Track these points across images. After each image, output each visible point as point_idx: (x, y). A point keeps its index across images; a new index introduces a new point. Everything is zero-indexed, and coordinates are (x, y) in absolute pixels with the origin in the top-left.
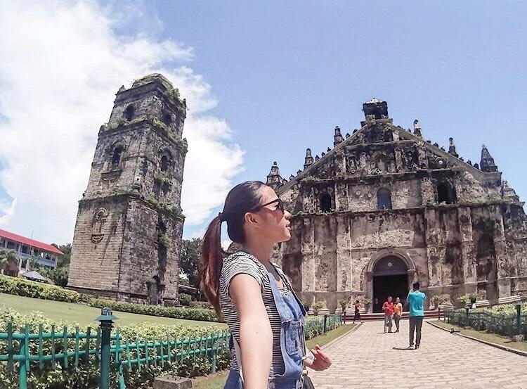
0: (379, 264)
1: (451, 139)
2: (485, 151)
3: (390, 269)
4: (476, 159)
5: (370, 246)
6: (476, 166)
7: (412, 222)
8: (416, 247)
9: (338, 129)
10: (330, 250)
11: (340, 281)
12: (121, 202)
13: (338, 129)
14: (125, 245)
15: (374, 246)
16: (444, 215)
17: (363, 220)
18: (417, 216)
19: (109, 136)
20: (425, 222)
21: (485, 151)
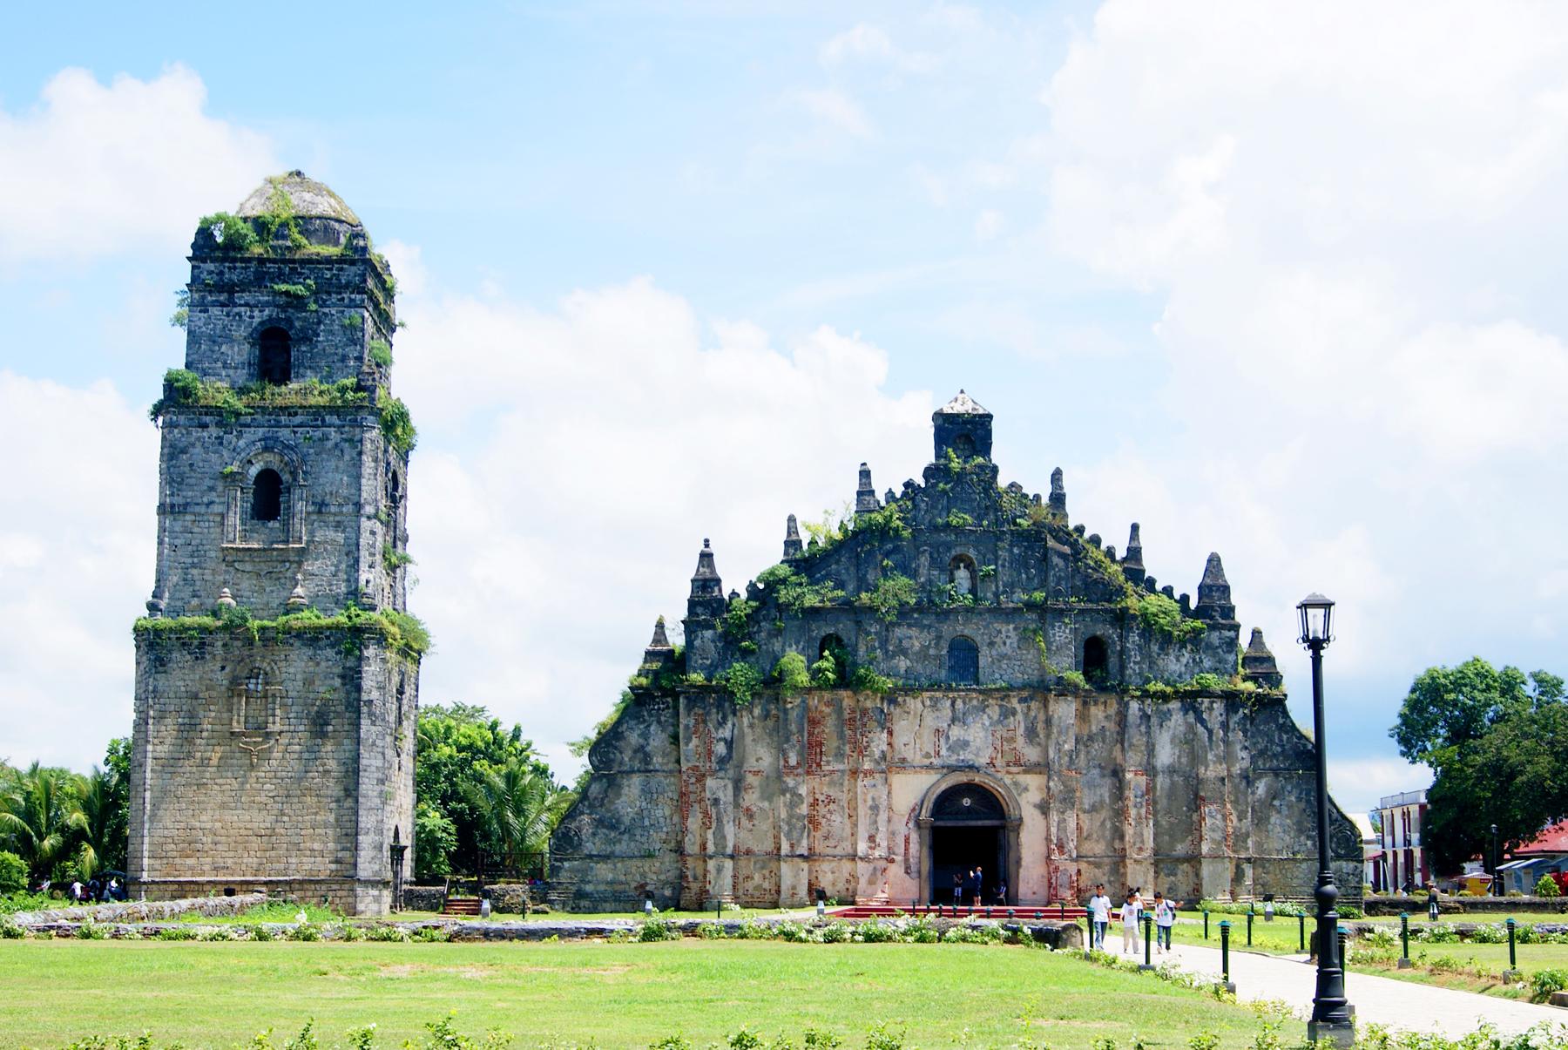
0: (945, 802)
1: (1135, 528)
2: (1214, 564)
3: (969, 811)
4: (1188, 584)
5: (927, 762)
6: (1185, 599)
7: (1020, 717)
8: (1026, 772)
9: (865, 474)
10: (841, 767)
11: (863, 833)
12: (332, 646)
13: (865, 474)
14: (363, 762)
15: (936, 761)
16: (1093, 709)
17: (914, 704)
18: (1034, 705)
20: (1048, 722)
21: (1214, 564)
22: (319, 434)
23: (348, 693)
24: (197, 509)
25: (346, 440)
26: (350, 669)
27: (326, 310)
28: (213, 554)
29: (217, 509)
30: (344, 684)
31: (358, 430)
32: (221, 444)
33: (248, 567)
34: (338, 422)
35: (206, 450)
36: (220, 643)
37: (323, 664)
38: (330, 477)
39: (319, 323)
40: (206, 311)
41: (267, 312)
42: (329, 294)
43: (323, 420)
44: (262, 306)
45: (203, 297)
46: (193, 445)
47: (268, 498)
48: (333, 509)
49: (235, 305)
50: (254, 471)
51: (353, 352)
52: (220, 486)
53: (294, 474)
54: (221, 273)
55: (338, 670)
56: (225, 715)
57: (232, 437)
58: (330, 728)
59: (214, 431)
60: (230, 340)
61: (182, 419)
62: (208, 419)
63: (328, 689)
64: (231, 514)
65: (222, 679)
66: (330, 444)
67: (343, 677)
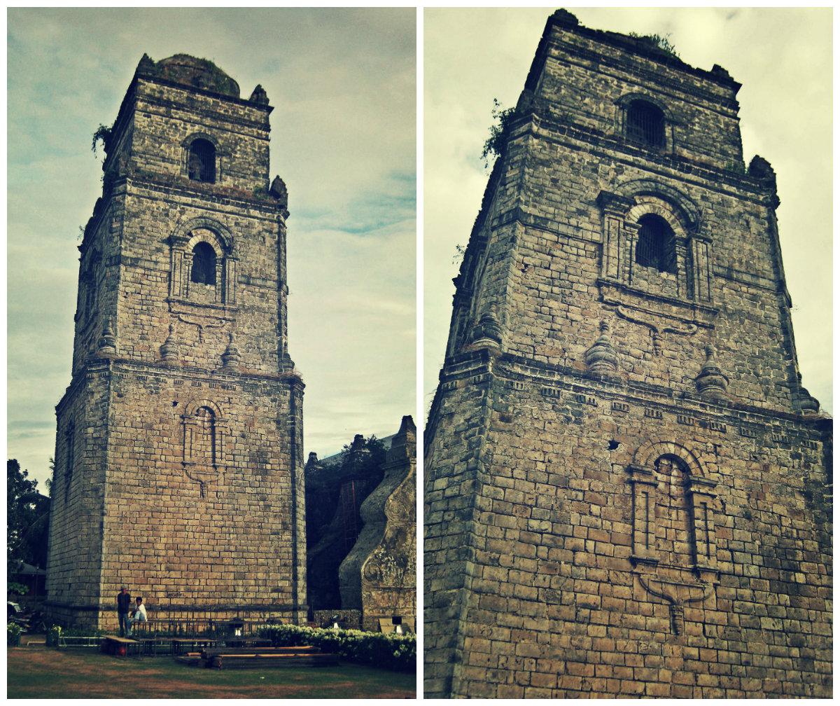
12: (269, 394)
19: (166, 201)
22: (245, 221)
23: (282, 436)
24: (147, 264)
25: (266, 231)
26: (284, 415)
27: (242, 136)
28: (160, 305)
29: (167, 267)
30: (278, 428)
31: (276, 225)
32: (167, 215)
33: (190, 319)
34: (260, 216)
35: (155, 218)
36: (170, 381)
37: (261, 409)
38: (256, 257)
39: (236, 144)
40: (149, 117)
41: (197, 127)
42: (243, 125)
43: (248, 212)
44: (194, 123)
45: (146, 107)
46: (144, 212)
47: (205, 265)
48: (259, 282)
49: (172, 118)
50: (193, 242)
51: (262, 171)
52: (166, 248)
53: (228, 249)
54: (161, 92)
55: (274, 415)
56: (178, 448)
57: (175, 211)
58: (269, 467)
59: (162, 205)
60: (169, 142)
61: (134, 190)
62: (156, 194)
63: (267, 434)
64: (177, 272)
65: (174, 413)
66: (254, 231)
67: (278, 422)
